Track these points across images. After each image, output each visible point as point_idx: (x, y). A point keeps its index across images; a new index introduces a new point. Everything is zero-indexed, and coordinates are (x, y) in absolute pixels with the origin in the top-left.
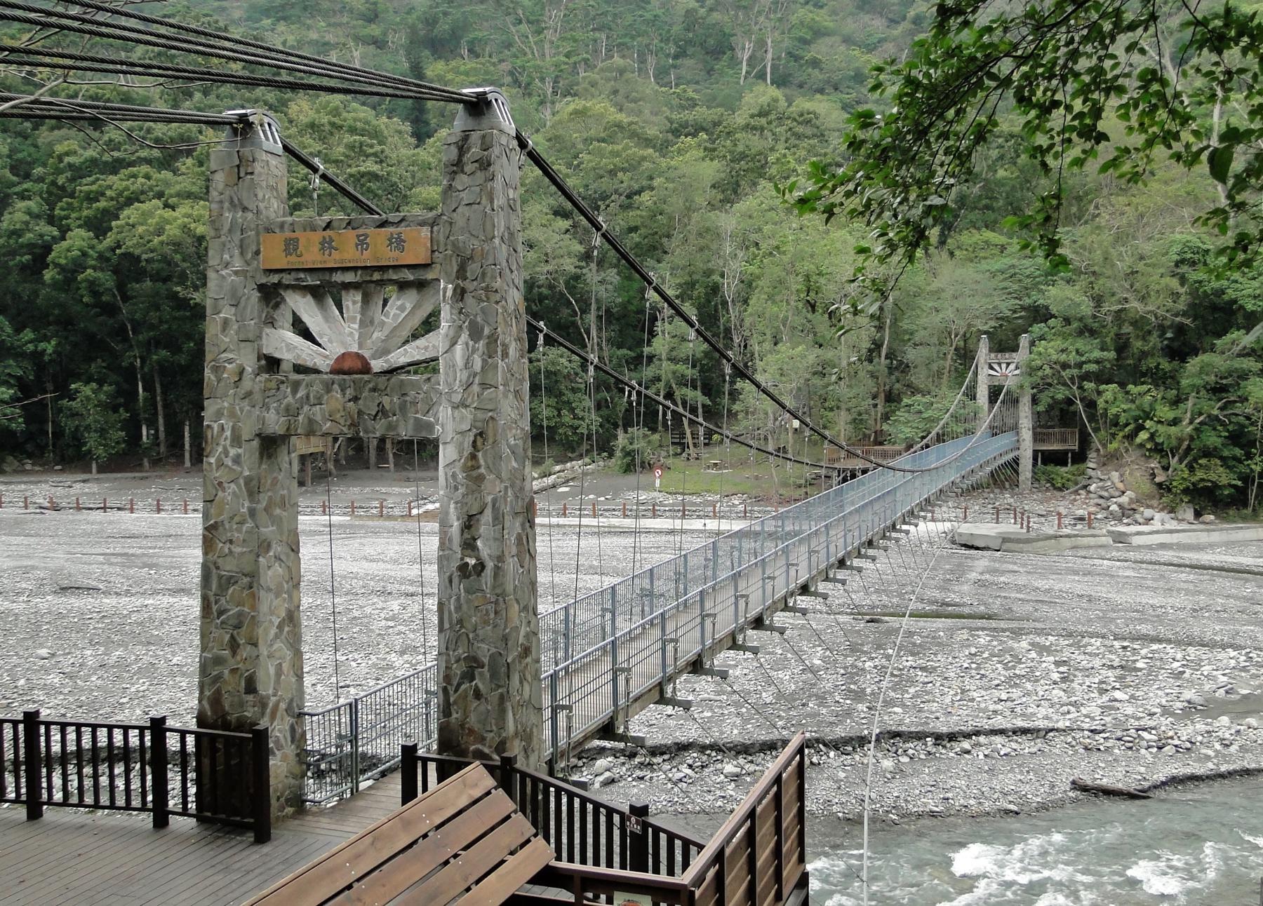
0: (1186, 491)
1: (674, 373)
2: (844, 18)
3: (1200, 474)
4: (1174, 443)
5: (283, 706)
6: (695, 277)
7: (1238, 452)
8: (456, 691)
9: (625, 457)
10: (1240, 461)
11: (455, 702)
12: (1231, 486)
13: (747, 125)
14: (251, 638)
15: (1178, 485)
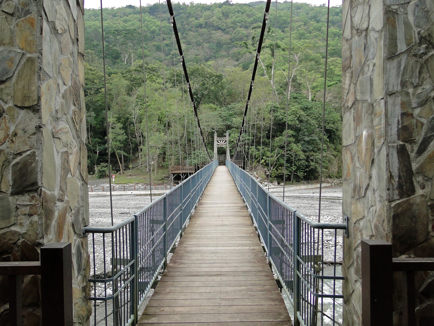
0: (276, 177)
1: (115, 145)
2: (152, 53)
3: (279, 171)
4: (272, 162)
5: (69, 219)
6: (121, 115)
7: (289, 165)
8: (420, 152)
9: (99, 173)
10: (289, 167)
11: (420, 171)
12: (288, 174)
13: (136, 70)
14: (26, 97)
15: (273, 175)
